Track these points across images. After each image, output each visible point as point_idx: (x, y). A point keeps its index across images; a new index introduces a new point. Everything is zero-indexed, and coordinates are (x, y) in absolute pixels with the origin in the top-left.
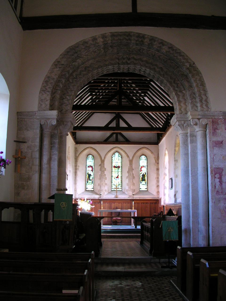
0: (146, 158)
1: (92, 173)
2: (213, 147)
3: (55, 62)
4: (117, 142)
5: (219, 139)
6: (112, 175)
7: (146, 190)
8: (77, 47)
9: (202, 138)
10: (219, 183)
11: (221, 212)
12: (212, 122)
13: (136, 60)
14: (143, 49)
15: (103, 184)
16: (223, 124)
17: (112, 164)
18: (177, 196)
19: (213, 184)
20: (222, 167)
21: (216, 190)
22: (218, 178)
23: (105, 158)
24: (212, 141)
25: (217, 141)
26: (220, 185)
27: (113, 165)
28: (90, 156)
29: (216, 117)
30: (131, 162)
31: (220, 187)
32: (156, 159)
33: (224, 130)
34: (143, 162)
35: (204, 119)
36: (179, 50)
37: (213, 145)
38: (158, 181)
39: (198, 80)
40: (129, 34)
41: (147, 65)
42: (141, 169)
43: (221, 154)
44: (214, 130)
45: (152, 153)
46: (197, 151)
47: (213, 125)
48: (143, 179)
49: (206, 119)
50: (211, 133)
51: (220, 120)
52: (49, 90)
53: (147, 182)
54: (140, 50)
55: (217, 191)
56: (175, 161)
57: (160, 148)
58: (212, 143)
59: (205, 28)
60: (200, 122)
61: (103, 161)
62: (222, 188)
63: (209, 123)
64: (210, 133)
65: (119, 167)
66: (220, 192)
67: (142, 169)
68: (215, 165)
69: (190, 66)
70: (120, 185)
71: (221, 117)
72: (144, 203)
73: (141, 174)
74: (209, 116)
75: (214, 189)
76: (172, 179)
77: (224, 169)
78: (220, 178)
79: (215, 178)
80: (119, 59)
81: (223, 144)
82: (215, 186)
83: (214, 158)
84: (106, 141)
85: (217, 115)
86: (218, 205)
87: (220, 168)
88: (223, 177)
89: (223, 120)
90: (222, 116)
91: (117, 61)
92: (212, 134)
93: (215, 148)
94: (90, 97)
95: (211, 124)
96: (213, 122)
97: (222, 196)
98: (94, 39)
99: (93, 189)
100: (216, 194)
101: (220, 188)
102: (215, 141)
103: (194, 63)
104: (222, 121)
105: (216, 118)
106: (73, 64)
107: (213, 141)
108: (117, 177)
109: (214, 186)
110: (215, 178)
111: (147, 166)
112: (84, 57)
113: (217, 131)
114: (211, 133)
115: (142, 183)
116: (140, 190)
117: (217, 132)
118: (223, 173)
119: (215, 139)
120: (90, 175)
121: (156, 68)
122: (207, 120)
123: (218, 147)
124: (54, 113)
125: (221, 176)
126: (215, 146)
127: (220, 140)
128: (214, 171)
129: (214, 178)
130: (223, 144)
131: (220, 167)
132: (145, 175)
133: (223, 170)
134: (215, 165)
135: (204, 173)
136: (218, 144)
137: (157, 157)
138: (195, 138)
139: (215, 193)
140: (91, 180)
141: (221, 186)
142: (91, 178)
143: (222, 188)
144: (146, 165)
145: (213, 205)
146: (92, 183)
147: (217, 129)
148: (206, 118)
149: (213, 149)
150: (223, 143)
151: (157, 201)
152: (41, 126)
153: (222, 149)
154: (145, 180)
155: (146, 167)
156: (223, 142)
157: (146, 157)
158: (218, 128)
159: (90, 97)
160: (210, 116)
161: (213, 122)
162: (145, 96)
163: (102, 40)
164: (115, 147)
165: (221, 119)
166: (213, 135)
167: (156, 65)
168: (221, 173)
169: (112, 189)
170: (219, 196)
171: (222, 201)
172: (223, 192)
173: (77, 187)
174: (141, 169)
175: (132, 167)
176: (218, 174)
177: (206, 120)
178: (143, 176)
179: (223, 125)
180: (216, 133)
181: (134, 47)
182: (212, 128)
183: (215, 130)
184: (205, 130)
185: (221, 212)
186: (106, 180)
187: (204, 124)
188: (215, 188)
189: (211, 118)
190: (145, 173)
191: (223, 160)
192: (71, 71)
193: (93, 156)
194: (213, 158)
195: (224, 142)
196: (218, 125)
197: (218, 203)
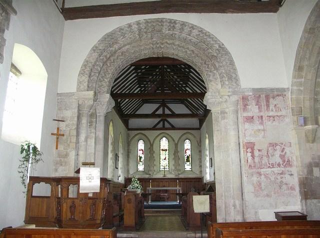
3: (93, 48)
4: (164, 128)
5: (250, 114)
8: (114, 34)
13: (169, 44)
14: (175, 34)
15: (152, 165)
21: (248, 165)
23: (153, 142)
27: (161, 148)
30: (176, 145)
34: (187, 145)
36: (209, 33)
39: (227, 59)
40: (161, 21)
41: (179, 49)
45: (195, 137)
48: (188, 161)
52: (87, 73)
54: (172, 35)
55: (250, 166)
59: (233, 12)
61: (152, 145)
62: (254, 162)
65: (166, 150)
68: (247, 140)
69: (220, 47)
71: (251, 94)
78: (252, 152)
79: (247, 152)
80: (153, 44)
84: (154, 128)
91: (152, 45)
94: (139, 89)
95: (242, 100)
97: (254, 170)
98: (130, 26)
103: (223, 45)
106: (111, 49)
107: (244, 117)
108: (165, 159)
112: (121, 42)
113: (248, 107)
119: (245, 114)
120: (141, 158)
121: (188, 51)
124: (91, 93)
131: (251, 141)
133: (254, 145)
137: (199, 140)
142: (142, 160)
143: (254, 162)
147: (247, 105)
149: (244, 124)
151: (200, 180)
152: (79, 106)
159: (139, 89)
161: (243, 98)
163: (137, 27)
167: (188, 48)
173: (129, 168)
175: (177, 150)
177: (236, 96)
178: (188, 157)
181: (167, 32)
183: (245, 105)
192: (108, 56)
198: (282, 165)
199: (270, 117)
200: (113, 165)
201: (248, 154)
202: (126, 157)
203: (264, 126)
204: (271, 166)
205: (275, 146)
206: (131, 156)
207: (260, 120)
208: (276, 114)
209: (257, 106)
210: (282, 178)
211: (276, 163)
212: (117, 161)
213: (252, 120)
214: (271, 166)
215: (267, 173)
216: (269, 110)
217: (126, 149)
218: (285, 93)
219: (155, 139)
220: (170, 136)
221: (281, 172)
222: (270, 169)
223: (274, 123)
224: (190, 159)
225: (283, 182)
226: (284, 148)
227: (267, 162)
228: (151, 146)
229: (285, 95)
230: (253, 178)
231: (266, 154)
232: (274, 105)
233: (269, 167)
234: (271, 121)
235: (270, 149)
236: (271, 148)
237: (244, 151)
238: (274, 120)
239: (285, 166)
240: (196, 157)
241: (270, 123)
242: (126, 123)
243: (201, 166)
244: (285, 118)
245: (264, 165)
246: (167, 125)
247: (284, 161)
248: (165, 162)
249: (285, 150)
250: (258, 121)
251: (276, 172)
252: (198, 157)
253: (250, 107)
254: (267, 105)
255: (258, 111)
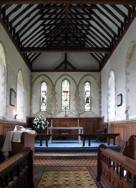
0: (90, 84)
1: (45, 97)
4: (66, 70)
6: (62, 98)
7: (90, 110)
17: (62, 89)
18: (129, 112)
23: (56, 83)
27: (63, 90)
28: (44, 83)
30: (77, 86)
32: (99, 84)
34: (87, 87)
38: (100, 103)
42: (85, 93)
45: (95, 79)
48: (87, 102)
53: (91, 104)
56: (126, 74)
57: (102, 75)
61: (54, 86)
65: (67, 92)
67: (87, 93)
70: (69, 107)
72: (88, 121)
73: (85, 97)
76: (121, 95)
84: (57, 69)
94: (43, 32)
99: (46, 110)
108: (66, 100)
111: (91, 91)
115: (86, 105)
116: (85, 110)
120: (43, 99)
132: (88, 98)
137: (99, 82)
140: (44, 103)
142: (45, 101)
144: (90, 90)
146: (46, 105)
151: (100, 120)
154: (88, 102)
155: (90, 91)
157: (90, 83)
162: (92, 19)
164: (65, 74)
169: (62, 110)
174: (85, 93)
175: (78, 91)
178: (88, 99)
186: (56, 102)
190: (89, 97)
193: (46, 83)
200: (5, 100)
202: (29, 97)
206: (34, 96)
212: (13, 97)
217: (29, 89)
219: (57, 81)
220: (72, 78)
224: (90, 100)
228: (53, 86)
240: (96, 98)
242: (29, 63)
243: (100, 107)
246: (69, 67)
248: (66, 103)
252: (98, 98)
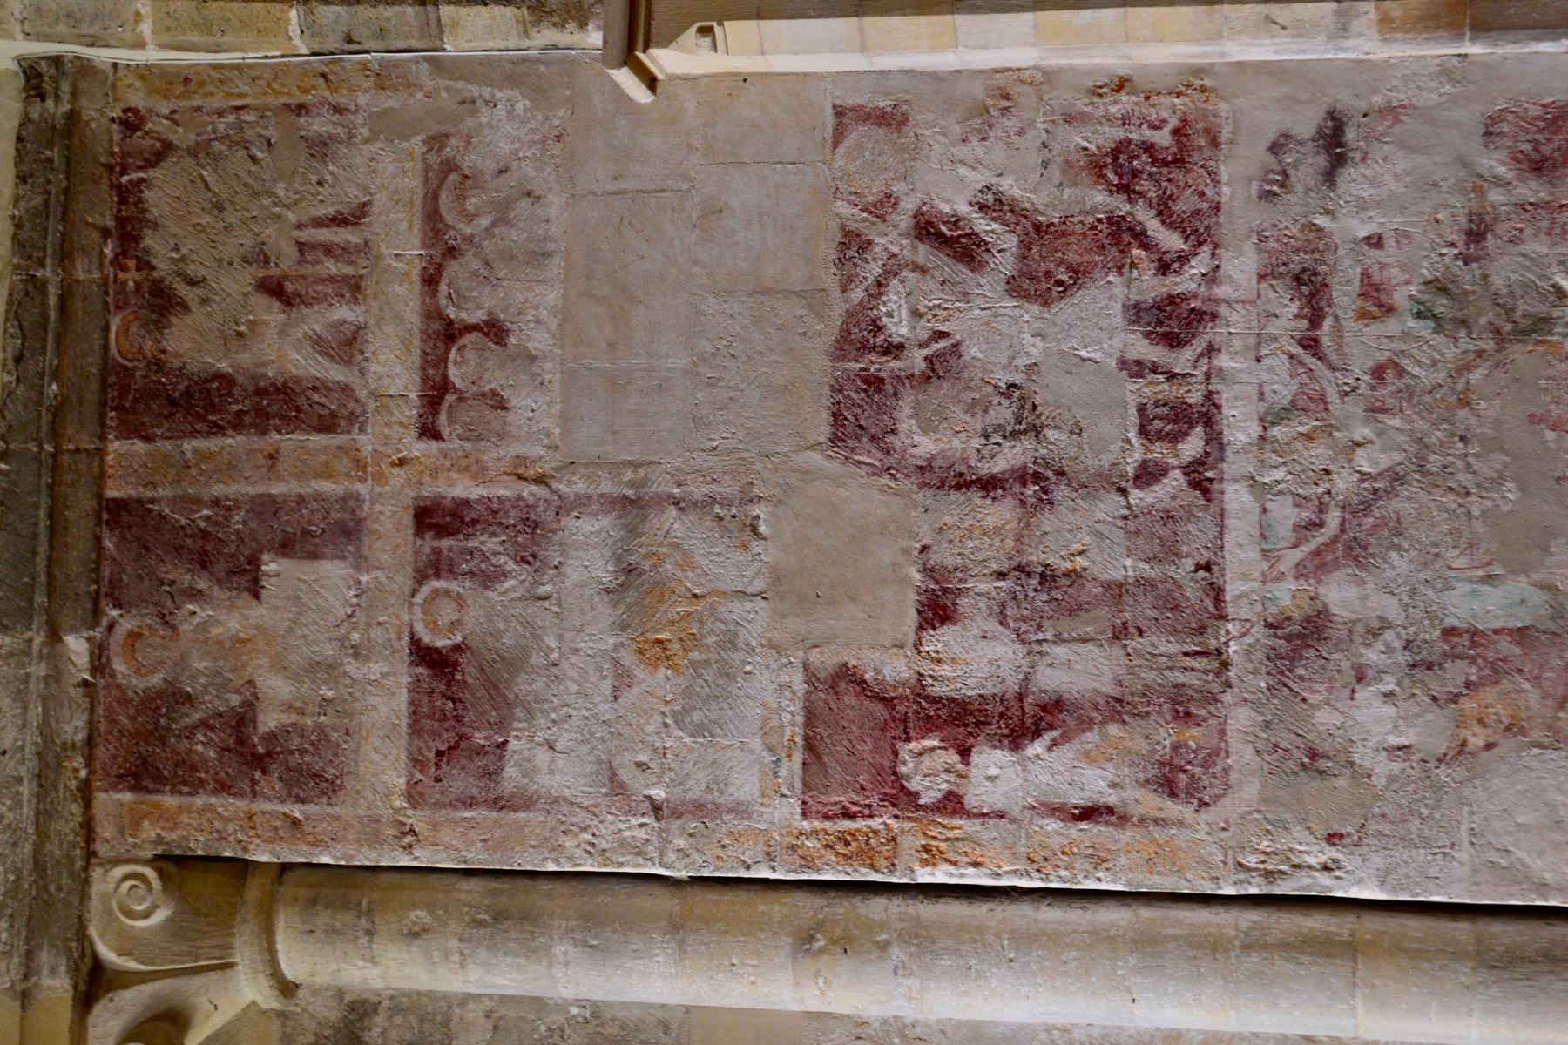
2: (499, 804)
9: (370, 933)
10: (1036, 748)
11: (1489, 746)
12: (136, 788)
16: (174, 628)
19: (1056, 843)
20: (800, 688)
21: (1150, 802)
22: (965, 753)
24: (418, 819)
25: (415, 730)
26: (1066, 738)
29: (74, 727)
31: (1092, 737)
33: (258, 613)
35: (95, 903)
37: (471, 803)
43: (606, 687)
44: (260, 762)
46: (563, 1007)
47: (187, 776)
49: (96, 873)
50: (297, 811)
51: (119, 666)
55: (1168, 781)
58: (442, 815)
60: (133, 965)
62: (1118, 708)
63: (149, 831)
64: (295, 823)
66: (1176, 748)
71: (77, 646)
74: (42, 833)
75: (1127, 835)
77: (826, 659)
81: (458, 639)
82: (1088, 813)
83: (658, 793)
85: (36, 711)
86: (1380, 781)
87: (811, 718)
88: (945, 670)
89: (126, 625)
90: (54, 636)
92: (311, 808)
93: (510, 771)
95: (169, 801)
96: (135, 775)
97: (1241, 719)
100: (1203, 804)
101: (1114, 729)
102: (417, 762)
104: (134, 636)
105: (80, 736)
107: (414, 796)
109: (1084, 825)
110: (969, 815)
113: (270, 720)
114: (297, 811)
117: (285, 731)
118: (888, 674)
122: (117, 862)
123: (502, 725)
125: (936, 700)
126: (492, 774)
127: (406, 679)
128: (851, 816)
129: (957, 822)
130: (457, 648)
133: (846, 676)
134: (763, 795)
135: (883, 947)
136: (459, 719)
138: (380, 1020)
139: (1186, 811)
141: (1086, 724)
143: (1118, 708)
145: (1377, 860)
147: (242, 720)
148: (86, 882)
149: (525, 802)
150: (441, 643)
153: (536, 659)
156: (427, 638)
158: (235, 700)
160: (43, 817)
165: (99, 664)
166: (329, 787)
168: (888, 702)
170: (1241, 754)
171: (1325, 718)
172: (1179, 686)
176: (905, 749)
177: (107, 883)
179: (185, 628)
180: (302, 732)
182: (223, 788)
184: (254, 890)
185: (1489, 746)
187: (159, 916)
188: (1110, 810)
189: (76, 809)
191: (694, 665)
194: (657, 808)
195: (432, 625)
196: (188, 699)
197: (1341, 783)
198: (1185, 281)
199: (436, 392)
201: (977, 794)
203: (582, 503)
204: (1193, 445)
205: (876, 364)
207: (488, 543)
208: (406, 297)
209: (271, 565)
210: (1374, 299)
211: (1136, 369)
213: (469, 671)
214: (1193, 445)
215: (1285, 514)
216: (346, 389)
218: (98, 114)
221: (1287, 309)
222: (1236, 497)
223: (539, 340)
225: (1439, 287)
226: (926, 229)
227: (1112, 504)
229: (132, 122)
230: (1363, 756)
231: (999, 513)
232: (271, 313)
233: (1200, 479)
234: (495, 379)
235: (926, 446)
236: (907, 425)
237: (930, 855)
238: (495, 331)
239: (1199, 232)
241: (523, 402)
244: (469, 162)
245: (1171, 552)
247: (1123, 234)
249: (956, 202)
250: (488, 578)
251: (1283, 389)
253: (275, 686)
254: (261, 421)
255: (332, 572)
